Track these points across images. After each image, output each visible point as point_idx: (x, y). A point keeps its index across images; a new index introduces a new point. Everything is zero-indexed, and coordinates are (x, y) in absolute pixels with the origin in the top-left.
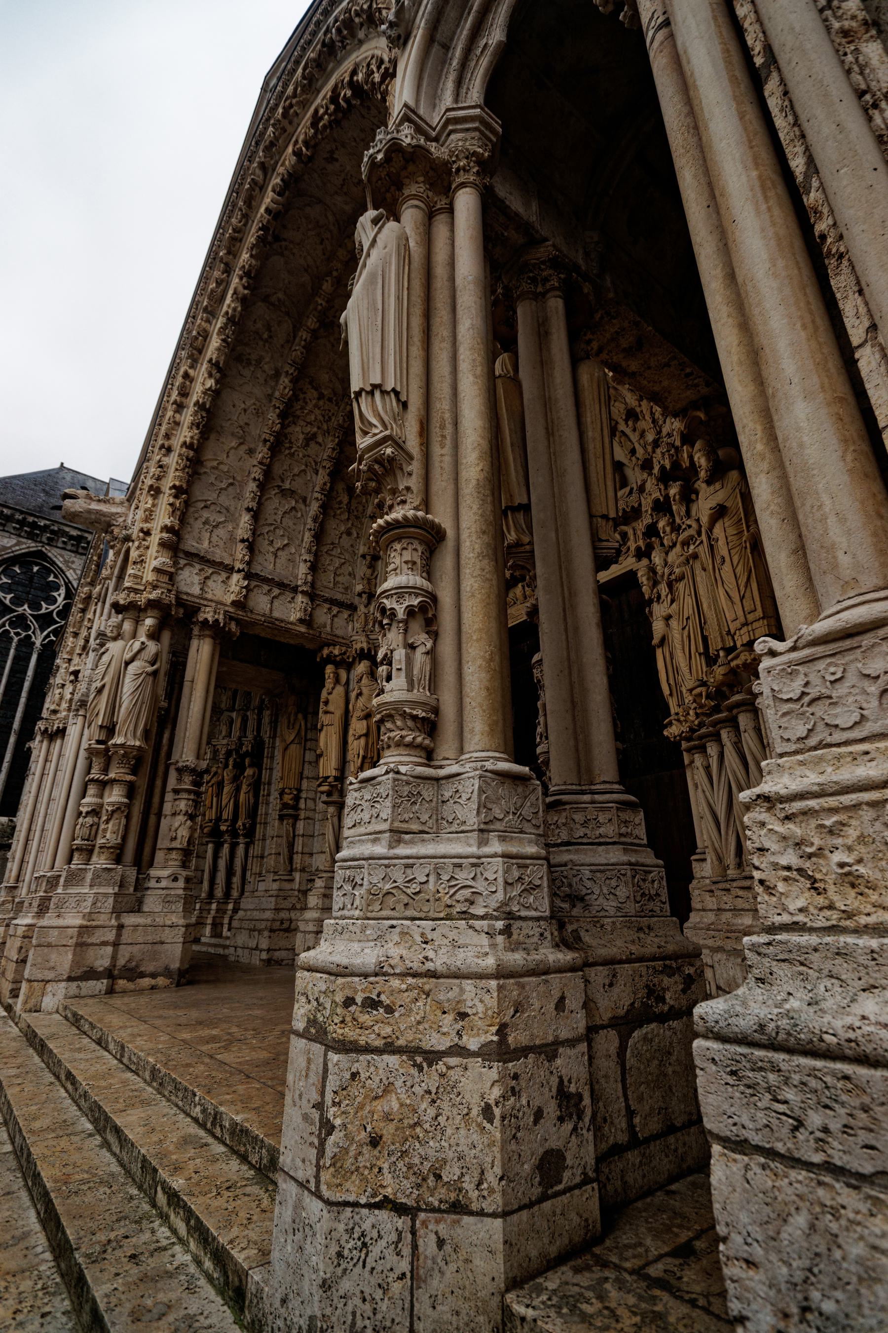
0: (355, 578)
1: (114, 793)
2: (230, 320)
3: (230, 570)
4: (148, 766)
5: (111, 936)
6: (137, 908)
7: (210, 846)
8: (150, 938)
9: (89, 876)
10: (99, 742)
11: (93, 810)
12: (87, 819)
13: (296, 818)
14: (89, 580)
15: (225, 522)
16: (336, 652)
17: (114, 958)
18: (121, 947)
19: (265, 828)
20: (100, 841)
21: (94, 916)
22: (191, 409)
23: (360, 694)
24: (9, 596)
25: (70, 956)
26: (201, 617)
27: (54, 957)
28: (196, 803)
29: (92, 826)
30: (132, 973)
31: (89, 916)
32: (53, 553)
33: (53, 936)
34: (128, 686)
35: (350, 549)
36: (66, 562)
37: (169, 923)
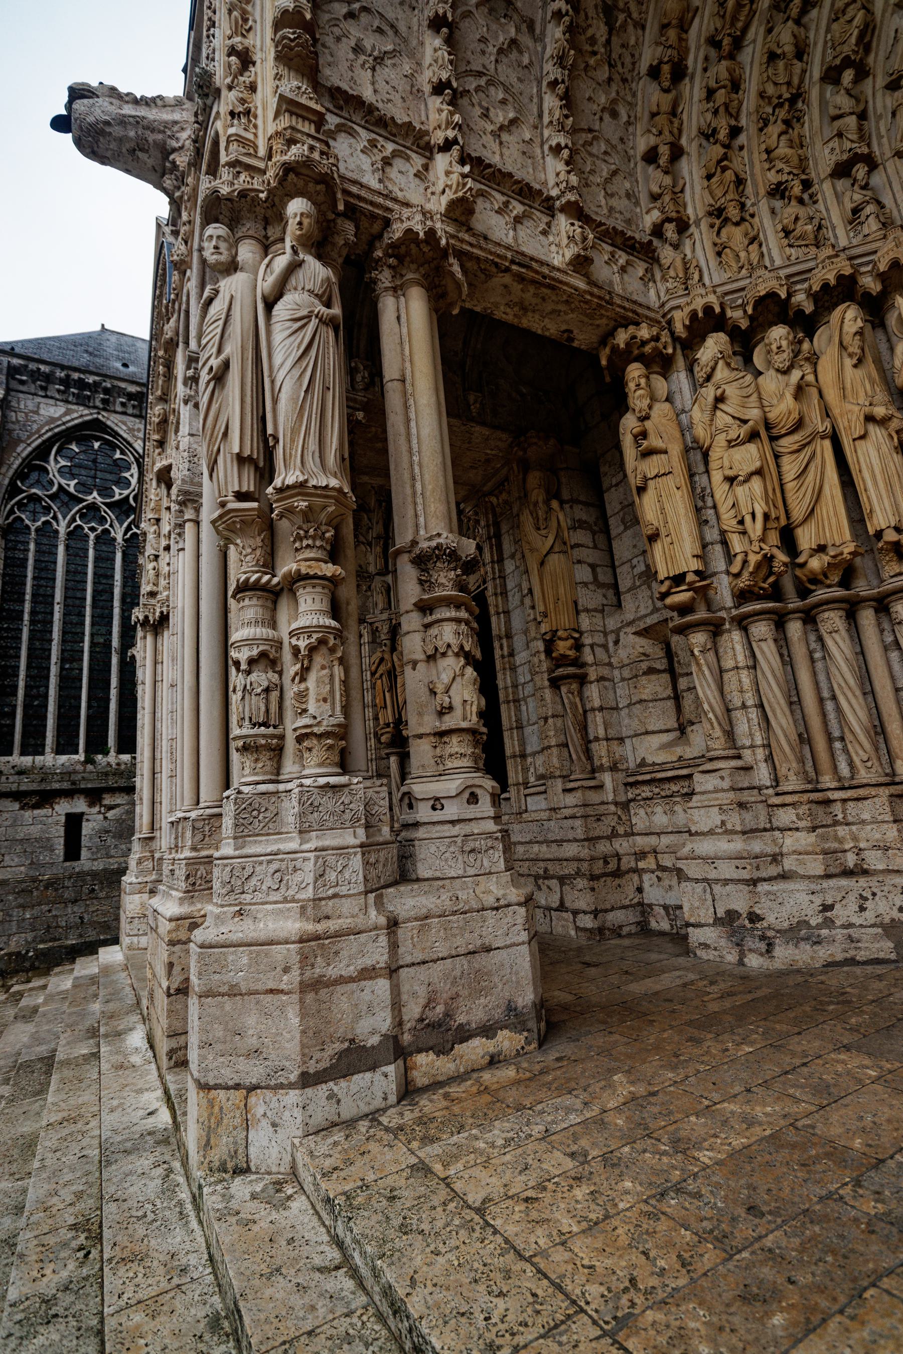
0: (637, 203)
1: (302, 607)
7: (393, 759)
8: (461, 943)
10: (241, 496)
11: (263, 655)
12: (254, 677)
13: (582, 680)
14: (159, 393)
15: (393, 54)
16: (644, 332)
17: (397, 1005)
18: (403, 972)
19: (518, 710)
20: (292, 724)
21: (328, 907)
23: (720, 399)
24: (73, 483)
25: (294, 1020)
26: (397, 231)
29: (267, 690)
30: (443, 1034)
31: (314, 908)
32: (112, 420)
34: (283, 347)
35: (620, 147)
36: (131, 430)
37: (490, 901)
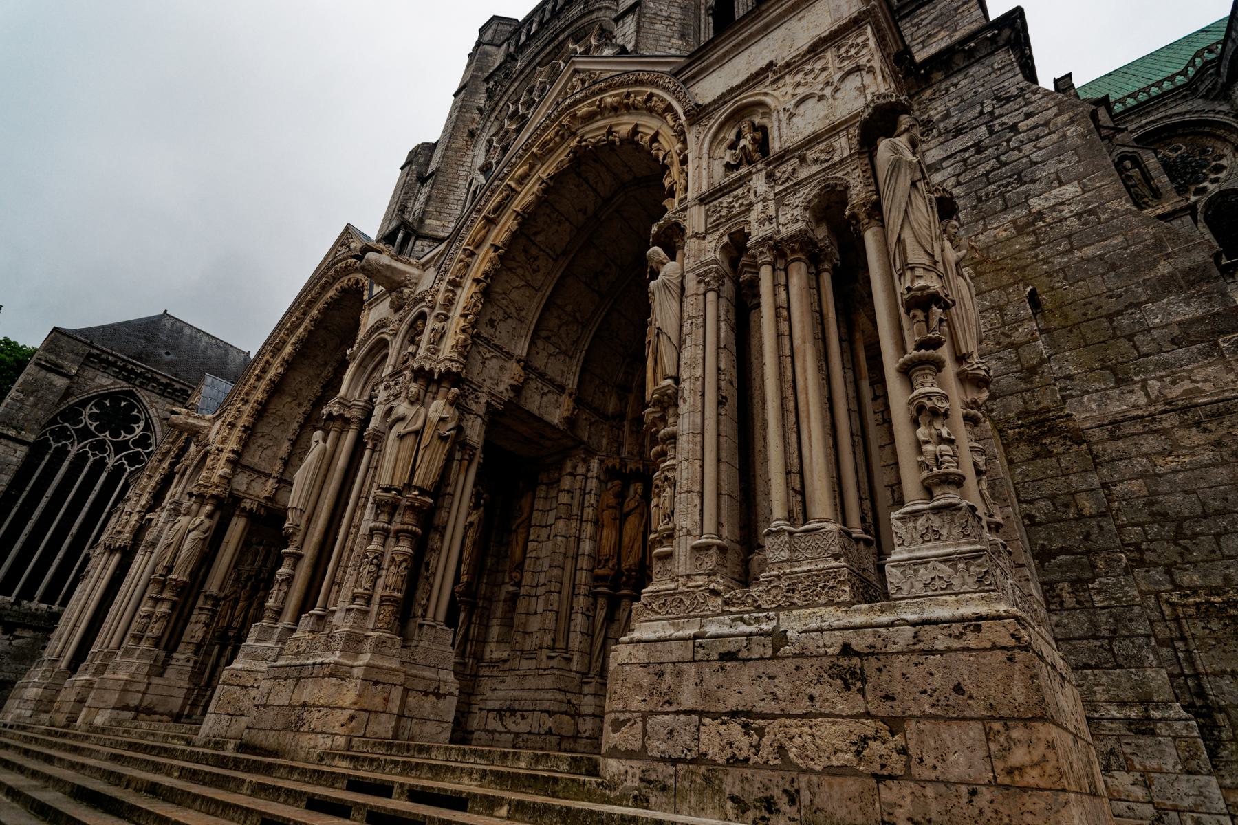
2: (300, 340)
3: (269, 476)
4: (187, 595)
5: (142, 688)
6: (161, 675)
8: (165, 693)
9: (138, 652)
17: (141, 700)
20: (148, 633)
22: (265, 382)
26: (243, 505)
27: (107, 696)
28: (212, 618)
31: (132, 675)
32: (142, 394)
33: (109, 684)
34: (187, 545)
36: (151, 402)
